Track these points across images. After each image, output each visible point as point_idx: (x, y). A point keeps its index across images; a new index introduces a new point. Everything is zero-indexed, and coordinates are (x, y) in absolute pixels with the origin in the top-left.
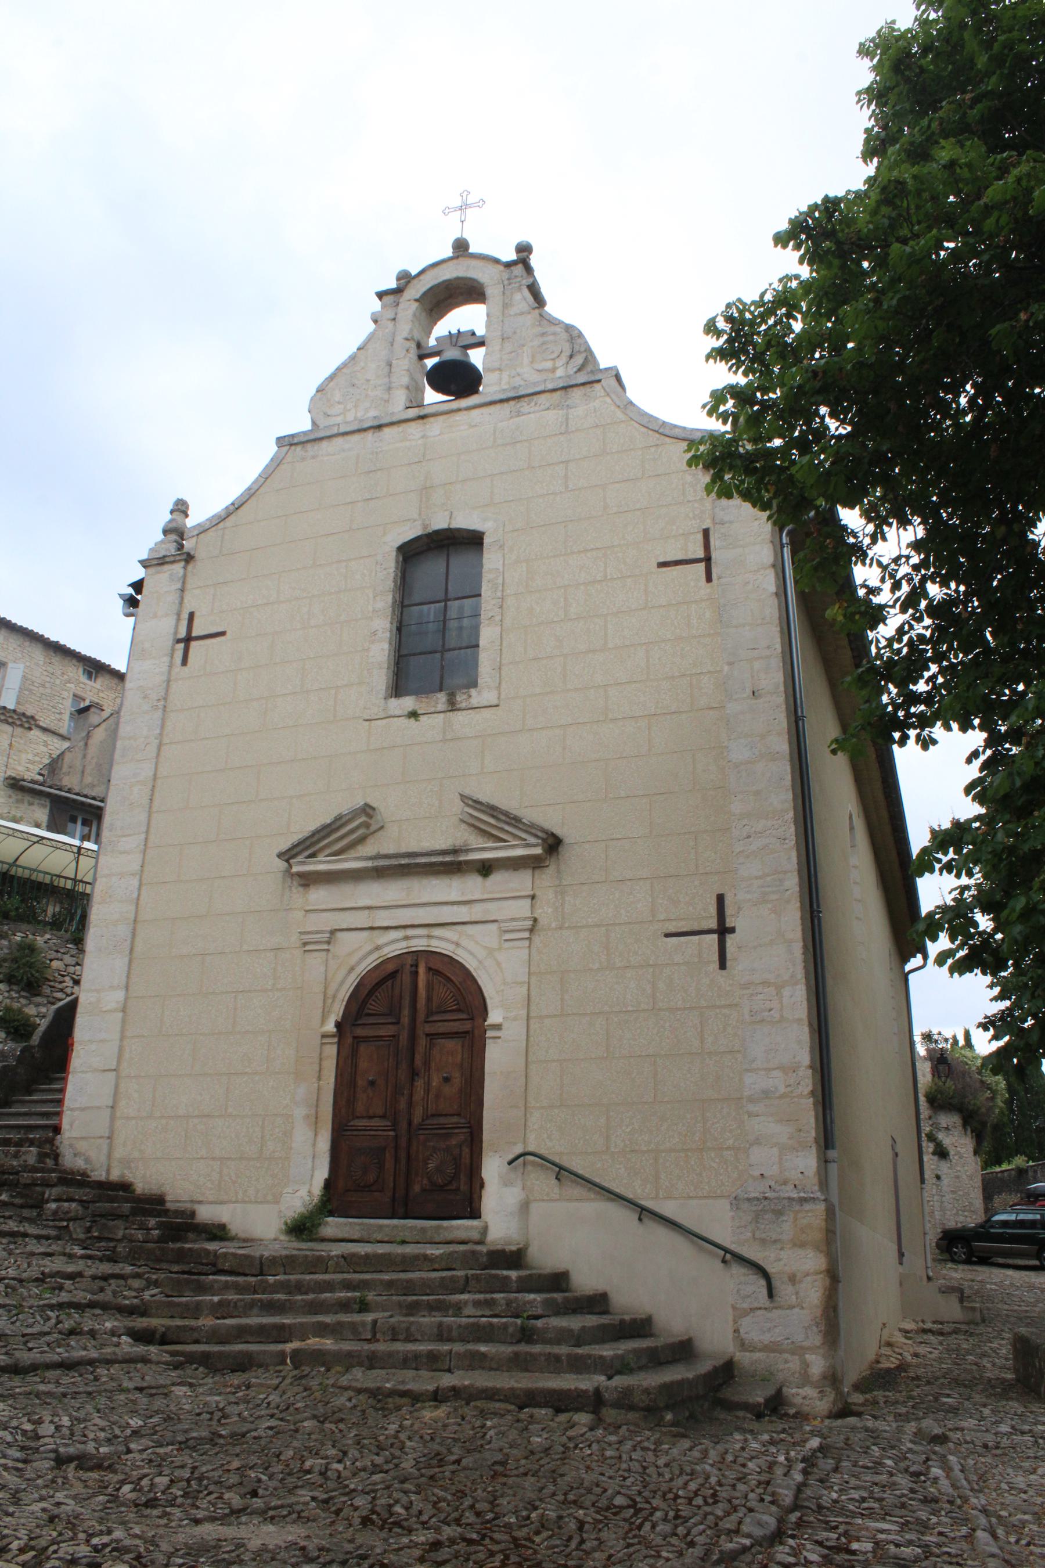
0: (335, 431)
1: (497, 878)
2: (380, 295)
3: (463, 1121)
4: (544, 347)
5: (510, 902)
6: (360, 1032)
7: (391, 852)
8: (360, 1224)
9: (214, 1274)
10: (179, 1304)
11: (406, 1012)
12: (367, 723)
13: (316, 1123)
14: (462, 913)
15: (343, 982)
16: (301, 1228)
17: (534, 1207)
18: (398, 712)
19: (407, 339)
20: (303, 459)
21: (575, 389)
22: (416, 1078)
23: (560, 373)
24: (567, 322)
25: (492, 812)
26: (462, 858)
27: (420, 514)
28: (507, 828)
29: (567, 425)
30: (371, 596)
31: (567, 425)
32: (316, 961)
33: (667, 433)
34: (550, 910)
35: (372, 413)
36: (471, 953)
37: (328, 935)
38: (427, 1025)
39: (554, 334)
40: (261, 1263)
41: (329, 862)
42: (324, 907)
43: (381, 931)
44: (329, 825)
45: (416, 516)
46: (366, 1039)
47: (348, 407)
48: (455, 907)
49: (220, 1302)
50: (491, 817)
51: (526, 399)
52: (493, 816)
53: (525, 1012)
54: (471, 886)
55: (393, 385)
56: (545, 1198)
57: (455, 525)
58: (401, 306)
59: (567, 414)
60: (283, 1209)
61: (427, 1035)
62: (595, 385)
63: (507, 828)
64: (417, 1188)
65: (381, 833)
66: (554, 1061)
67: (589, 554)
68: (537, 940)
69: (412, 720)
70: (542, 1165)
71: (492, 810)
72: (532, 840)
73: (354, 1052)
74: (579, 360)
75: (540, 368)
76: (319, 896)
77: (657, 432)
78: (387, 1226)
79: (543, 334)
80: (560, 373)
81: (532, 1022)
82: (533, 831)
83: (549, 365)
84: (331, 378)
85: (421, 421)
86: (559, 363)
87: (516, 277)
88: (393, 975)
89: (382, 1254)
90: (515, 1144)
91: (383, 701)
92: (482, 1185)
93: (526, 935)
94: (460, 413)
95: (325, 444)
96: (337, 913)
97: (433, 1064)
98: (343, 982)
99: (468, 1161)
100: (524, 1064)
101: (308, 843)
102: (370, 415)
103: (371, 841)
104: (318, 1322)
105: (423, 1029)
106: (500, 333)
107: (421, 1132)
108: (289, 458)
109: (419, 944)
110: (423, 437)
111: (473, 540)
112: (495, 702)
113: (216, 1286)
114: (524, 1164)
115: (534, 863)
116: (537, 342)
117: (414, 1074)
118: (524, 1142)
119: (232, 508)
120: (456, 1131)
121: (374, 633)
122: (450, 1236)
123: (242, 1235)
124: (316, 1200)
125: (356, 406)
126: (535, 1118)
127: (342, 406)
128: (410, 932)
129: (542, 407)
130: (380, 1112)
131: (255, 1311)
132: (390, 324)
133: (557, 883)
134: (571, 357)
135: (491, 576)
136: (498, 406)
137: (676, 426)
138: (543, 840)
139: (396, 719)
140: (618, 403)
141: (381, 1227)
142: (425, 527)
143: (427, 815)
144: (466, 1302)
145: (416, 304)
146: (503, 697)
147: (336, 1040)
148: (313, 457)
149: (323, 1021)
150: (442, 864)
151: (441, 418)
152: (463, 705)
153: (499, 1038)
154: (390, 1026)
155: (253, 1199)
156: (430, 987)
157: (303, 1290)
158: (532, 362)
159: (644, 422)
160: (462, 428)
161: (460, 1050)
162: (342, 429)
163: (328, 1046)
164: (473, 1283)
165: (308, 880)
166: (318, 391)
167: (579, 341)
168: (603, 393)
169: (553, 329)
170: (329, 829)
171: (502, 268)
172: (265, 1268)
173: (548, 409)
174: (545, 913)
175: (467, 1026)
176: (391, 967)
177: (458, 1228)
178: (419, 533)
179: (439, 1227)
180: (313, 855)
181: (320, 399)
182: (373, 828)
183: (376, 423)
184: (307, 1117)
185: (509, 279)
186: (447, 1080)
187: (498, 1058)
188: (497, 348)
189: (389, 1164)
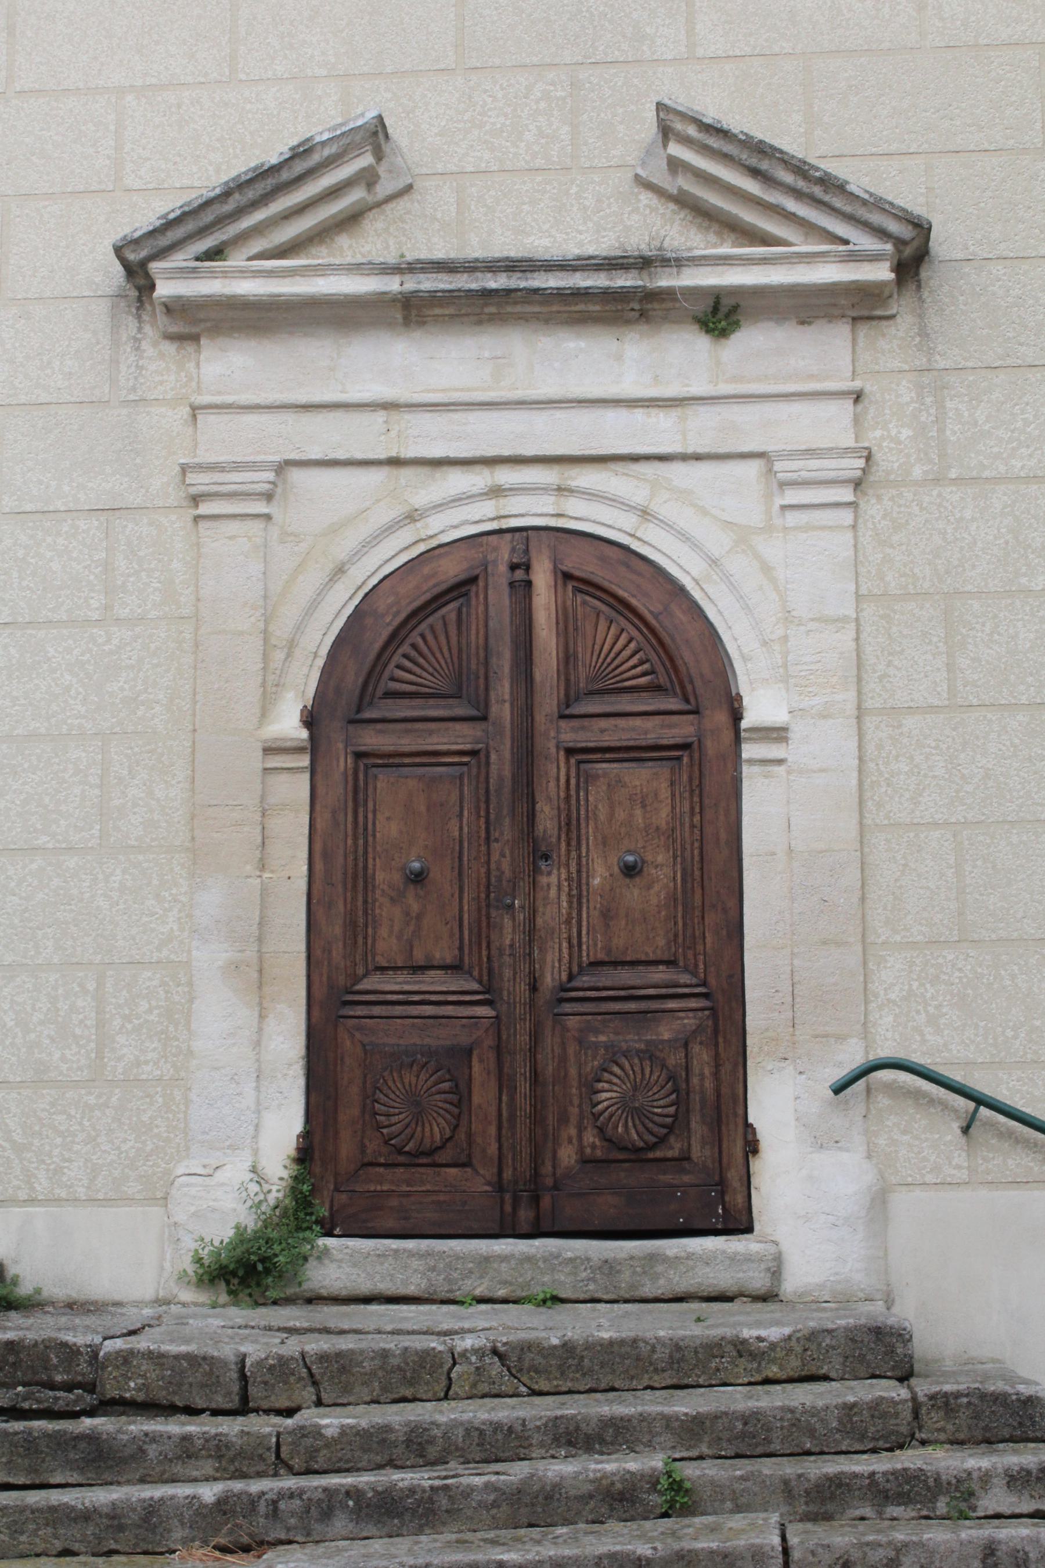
1: (752, 341)
3: (685, 978)
5: (797, 407)
6: (372, 739)
7: (439, 254)
8: (429, 1254)
9: (91, 1413)
10: (86, 1516)
11: (503, 689)
13: (260, 987)
14: (660, 431)
15: (314, 605)
16: (245, 1272)
17: (901, 1201)
22: (543, 865)
25: (753, 162)
26: (665, 281)
28: (791, 205)
32: (231, 546)
34: (906, 433)
36: (684, 537)
37: (270, 476)
38: (563, 723)
40: (243, 1377)
41: (270, 274)
42: (245, 398)
43: (423, 471)
44: (274, 170)
46: (392, 760)
48: (639, 414)
49: (223, 1506)
50: (736, 174)
52: (755, 173)
53: (851, 695)
54: (678, 358)
56: (929, 1178)
60: (180, 1217)
61: (570, 752)
63: (791, 205)
64: (567, 1155)
65: (401, 205)
66: (936, 825)
68: (872, 508)
70: (917, 1095)
71: (758, 157)
72: (864, 242)
73: (358, 795)
76: (230, 366)
78: (504, 1258)
81: (870, 723)
82: (876, 218)
88: (463, 587)
89: (611, 1343)
90: (841, 1038)
92: (752, 1147)
93: (846, 494)
96: (290, 417)
97: (590, 831)
98: (314, 605)
99: (709, 1084)
100: (854, 833)
101: (208, 217)
103: (374, 224)
104: (612, 1556)
105: (554, 736)
107: (567, 1007)
109: (532, 510)
113: (152, 1451)
114: (868, 1090)
115: (858, 307)
117: (538, 854)
118: (866, 1034)
120: (672, 1004)
122: (683, 1284)
123: (53, 1290)
124: (276, 1192)
126: (891, 974)
128: (506, 476)
130: (444, 953)
131: (341, 1523)
133: (921, 361)
138: (899, 243)
141: (487, 1260)
143: (540, 162)
144: (986, 1478)
147: (305, 761)
149: (265, 711)
150: (607, 295)
153: (780, 762)
154: (458, 726)
155: (81, 1192)
156: (567, 625)
157: (433, 1452)
161: (665, 793)
163: (284, 777)
164: (934, 1419)
165: (196, 324)
170: (270, 182)
172: (253, 1391)
174: (893, 438)
175: (681, 730)
176: (451, 570)
177: (707, 1260)
179: (652, 1258)
180: (216, 254)
182: (383, 189)
184: (235, 967)
186: (630, 871)
187: (775, 814)
189: (483, 1095)
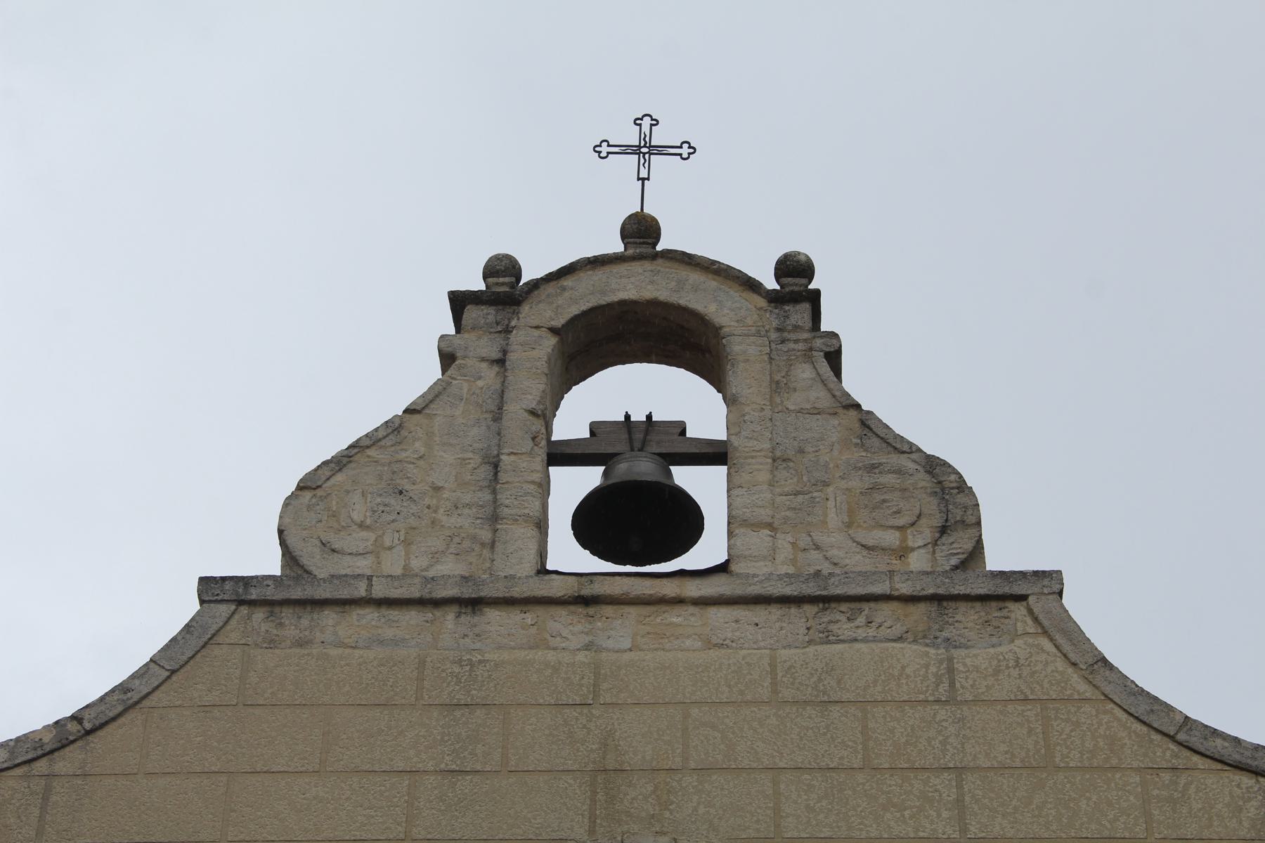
0: (361, 591)
2: (459, 302)
19: (532, 413)
20: (272, 643)
21: (963, 606)
23: (918, 561)
29: (952, 684)
33: (1195, 741)
35: (449, 567)
39: (899, 472)
47: (388, 543)
55: (505, 511)
58: (517, 337)
62: (1012, 606)
75: (870, 543)
77: (1172, 738)
79: (872, 468)
80: (918, 561)
85: (580, 609)
86: (915, 540)
87: (796, 328)
94: (678, 609)
95: (329, 617)
106: (767, 445)
108: (233, 634)
110: (588, 647)
119: (73, 727)
125: (407, 543)
127: (372, 536)
129: (884, 632)
132: (490, 375)
134: (943, 530)
136: (775, 611)
137: (1215, 732)
140: (1072, 656)
145: (552, 341)
148: (300, 643)
151: (633, 611)
158: (849, 525)
159: (1140, 710)
160: (688, 643)
162: (379, 591)
166: (300, 488)
167: (961, 499)
168: (1031, 627)
169: (895, 460)
171: (762, 302)
173: (899, 639)
181: (309, 508)
183: (468, 592)
185: (778, 330)
188: (764, 476)
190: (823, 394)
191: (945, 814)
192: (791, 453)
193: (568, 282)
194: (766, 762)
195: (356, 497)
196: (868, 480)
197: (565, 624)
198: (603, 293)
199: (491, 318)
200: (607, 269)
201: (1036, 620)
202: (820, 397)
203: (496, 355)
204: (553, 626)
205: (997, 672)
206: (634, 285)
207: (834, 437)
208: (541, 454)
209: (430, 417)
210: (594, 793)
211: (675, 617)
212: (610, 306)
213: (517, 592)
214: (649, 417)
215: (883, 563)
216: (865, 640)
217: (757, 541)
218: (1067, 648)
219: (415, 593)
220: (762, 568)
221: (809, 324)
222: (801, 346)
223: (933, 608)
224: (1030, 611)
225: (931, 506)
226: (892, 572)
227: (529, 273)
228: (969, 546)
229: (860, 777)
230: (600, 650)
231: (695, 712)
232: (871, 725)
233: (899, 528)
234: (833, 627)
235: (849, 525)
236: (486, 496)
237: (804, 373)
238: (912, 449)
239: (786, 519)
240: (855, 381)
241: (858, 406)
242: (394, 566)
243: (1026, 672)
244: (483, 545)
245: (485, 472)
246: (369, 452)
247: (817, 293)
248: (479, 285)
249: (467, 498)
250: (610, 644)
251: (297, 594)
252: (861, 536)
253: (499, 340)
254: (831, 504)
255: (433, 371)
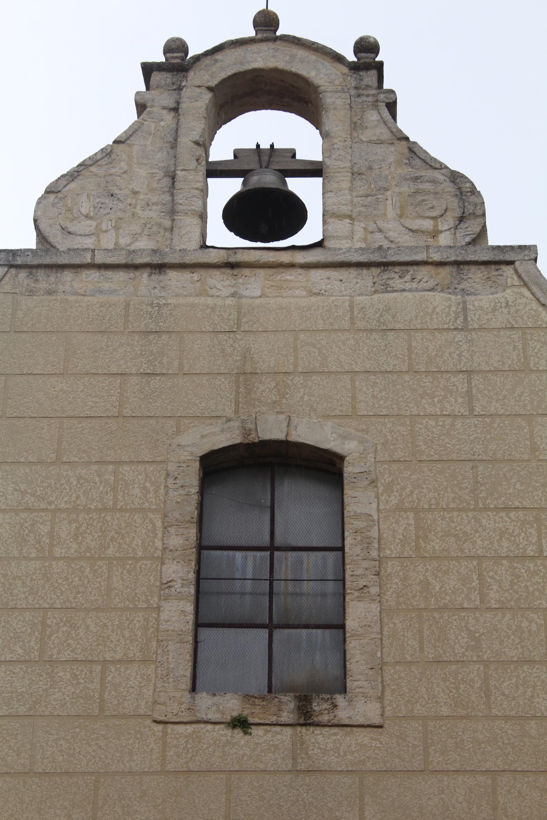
0: (88, 259)
2: (148, 69)
4: (420, 198)
12: (161, 727)
18: (213, 716)
19: (197, 143)
20: (31, 292)
21: (473, 268)
23: (444, 239)
24: (453, 168)
27: (236, 412)
29: (465, 318)
30: (159, 524)
31: (465, 318)
35: (144, 244)
39: (433, 181)
45: (229, 412)
47: (104, 228)
51: (397, 269)
57: (294, 437)
58: (186, 93)
59: (465, 303)
67: (512, 514)
69: (238, 733)
74: (474, 228)
75: (414, 227)
79: (416, 179)
80: (444, 239)
83: (428, 225)
84: (73, 175)
85: (228, 271)
86: (443, 226)
87: (368, 87)
91: (187, 695)
95: (68, 275)
102: (144, 246)
106: (348, 164)
110: (233, 295)
111: (324, 468)
112: (377, 720)
116: (405, 189)
121: (169, 584)
125: (117, 228)
127: (94, 223)
129: (422, 285)
132: (169, 118)
134: (461, 219)
135: (359, 524)
136: (353, 272)
139: (210, 727)
140: (542, 300)
142: (246, 433)
146: (387, 714)
148: (50, 293)
151: (262, 272)
152: (325, 718)
158: (401, 216)
160: (297, 292)
162: (99, 259)
166: (49, 191)
167: (473, 199)
168: (516, 282)
171: (345, 70)
173: (432, 289)
178: (238, 441)
181: (53, 205)
183: (156, 260)
185: (356, 88)
188: (346, 184)
190: (384, 130)
191: (460, 400)
192: (363, 169)
193: (219, 56)
194: (347, 368)
195: (84, 198)
196: (413, 187)
197: (219, 281)
198: (242, 63)
199: (169, 81)
200: (245, 47)
201: (520, 277)
202: (383, 133)
203: (172, 105)
204: (211, 282)
205: (494, 310)
206: (262, 59)
207: (391, 159)
208: (203, 170)
209: (131, 146)
210: (238, 387)
211: (289, 275)
212: (246, 72)
213: (188, 260)
214: (272, 146)
215: (422, 241)
216: (410, 290)
217: (341, 227)
218: (539, 294)
219: (122, 260)
220: (345, 244)
221: (376, 84)
222: (370, 99)
223: (454, 269)
224: (516, 271)
225: (454, 203)
226: (428, 247)
227: (195, 49)
228: (478, 229)
229: (407, 377)
230: (241, 297)
231: (302, 336)
232: (414, 344)
233: (433, 218)
234: (390, 282)
235: (401, 216)
236: (168, 198)
237: (372, 116)
238: (442, 167)
239: (360, 212)
240: (405, 122)
241: (407, 139)
242: (109, 243)
243: (512, 310)
244: (166, 229)
245: (166, 182)
246: (92, 169)
247: (381, 64)
248: (160, 58)
249: (155, 199)
250: (247, 293)
251: (47, 260)
252: (409, 223)
253: (175, 95)
254: (389, 202)
255: (132, 116)
